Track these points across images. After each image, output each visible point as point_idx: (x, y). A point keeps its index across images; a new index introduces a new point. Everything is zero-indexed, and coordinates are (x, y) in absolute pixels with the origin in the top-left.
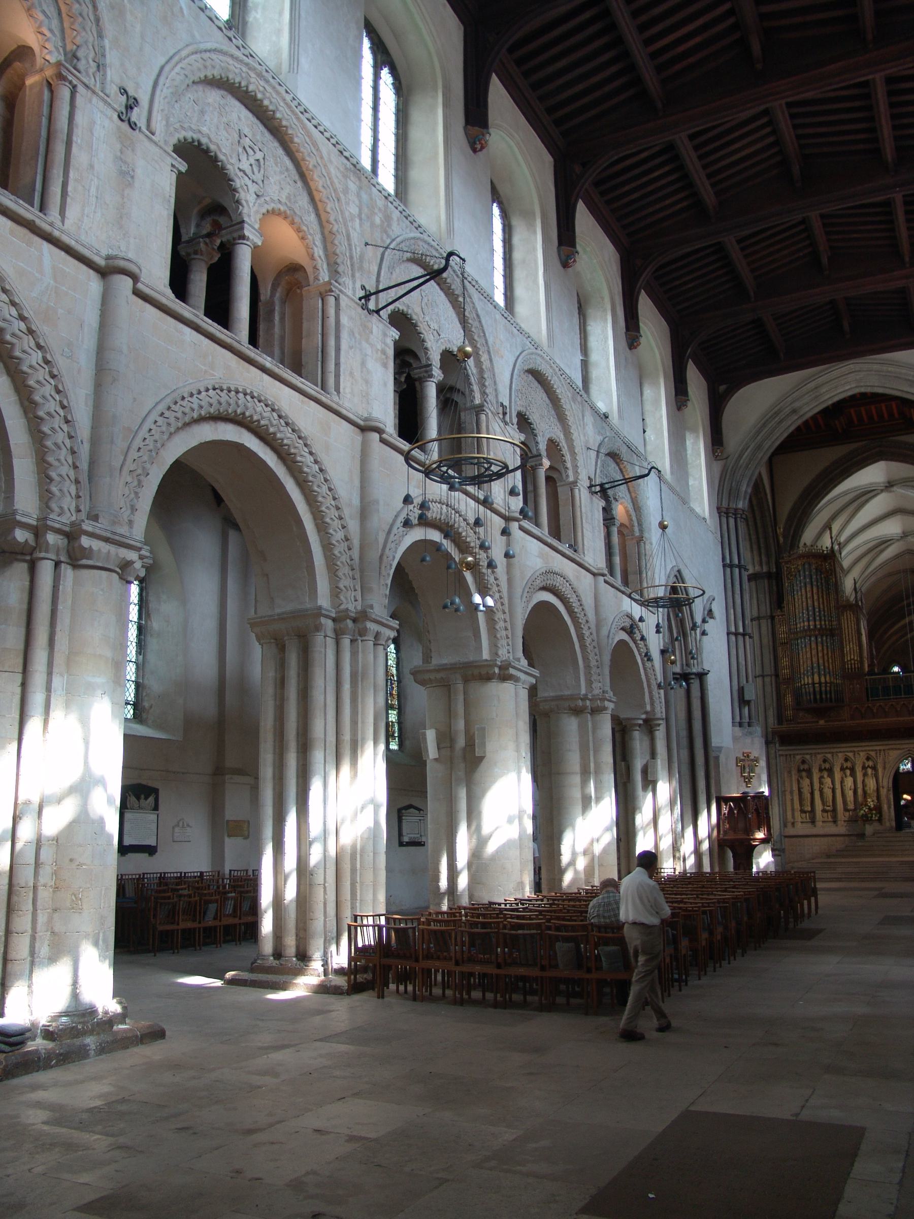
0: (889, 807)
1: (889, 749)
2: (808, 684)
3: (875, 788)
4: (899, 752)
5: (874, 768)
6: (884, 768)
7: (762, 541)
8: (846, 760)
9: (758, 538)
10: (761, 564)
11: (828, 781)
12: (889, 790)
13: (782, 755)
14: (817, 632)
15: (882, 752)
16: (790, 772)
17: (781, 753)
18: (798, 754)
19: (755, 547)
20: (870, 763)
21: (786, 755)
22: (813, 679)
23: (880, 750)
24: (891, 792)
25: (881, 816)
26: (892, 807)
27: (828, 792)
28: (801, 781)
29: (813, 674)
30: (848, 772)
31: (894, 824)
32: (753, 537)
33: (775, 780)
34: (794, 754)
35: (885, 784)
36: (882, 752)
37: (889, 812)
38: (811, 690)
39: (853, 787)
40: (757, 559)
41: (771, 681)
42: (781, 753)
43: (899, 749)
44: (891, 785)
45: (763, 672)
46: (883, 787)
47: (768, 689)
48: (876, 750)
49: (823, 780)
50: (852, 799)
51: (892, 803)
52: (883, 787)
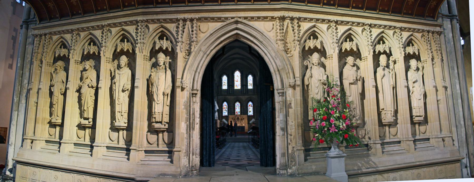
0: (190, 128)
1: (199, 19)
3: (169, 91)
4: (219, 25)
5: (172, 54)
6: (189, 53)
8: (124, 38)
11: (92, 74)
12: (194, 95)
15: (188, 23)
20: (165, 44)
23: (185, 20)
24: (198, 99)
25: (171, 143)
26: (197, 127)
27: (88, 94)
28: (54, 75)
30: (124, 60)
31: (197, 160)
35: (187, 82)
36: (188, 23)
37: (190, 136)
39: (129, 87)
43: (219, 19)
44: (198, 86)
46: (183, 89)
48: (178, 20)
49: (84, 73)
50: (125, 108)
51: (198, 120)
52: (183, 89)
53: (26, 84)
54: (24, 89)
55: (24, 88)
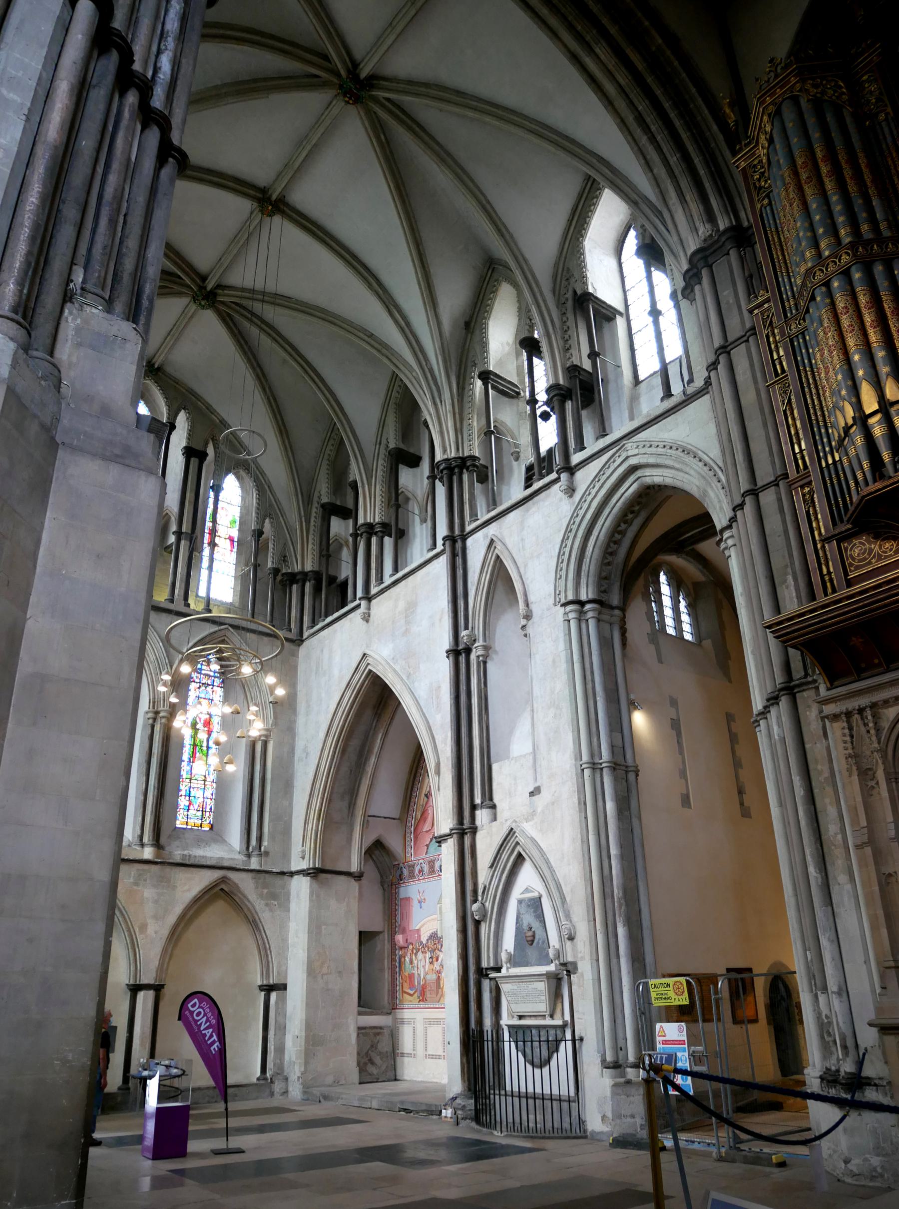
2: (847, 429)
7: (697, 161)
9: (686, 158)
10: (711, 218)
13: (835, 717)
14: (845, 258)
16: (865, 774)
17: (830, 709)
18: (886, 703)
19: (685, 183)
21: (848, 714)
22: (858, 405)
29: (855, 390)
32: (673, 160)
33: (832, 811)
34: (873, 706)
38: (859, 440)
40: (695, 207)
41: (780, 500)
42: (830, 709)
45: (756, 485)
47: (773, 523)
53: (836, 834)
54: (833, 847)
55: (835, 845)
